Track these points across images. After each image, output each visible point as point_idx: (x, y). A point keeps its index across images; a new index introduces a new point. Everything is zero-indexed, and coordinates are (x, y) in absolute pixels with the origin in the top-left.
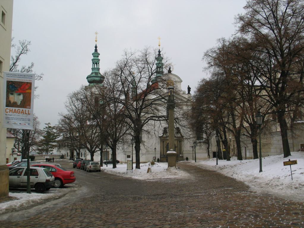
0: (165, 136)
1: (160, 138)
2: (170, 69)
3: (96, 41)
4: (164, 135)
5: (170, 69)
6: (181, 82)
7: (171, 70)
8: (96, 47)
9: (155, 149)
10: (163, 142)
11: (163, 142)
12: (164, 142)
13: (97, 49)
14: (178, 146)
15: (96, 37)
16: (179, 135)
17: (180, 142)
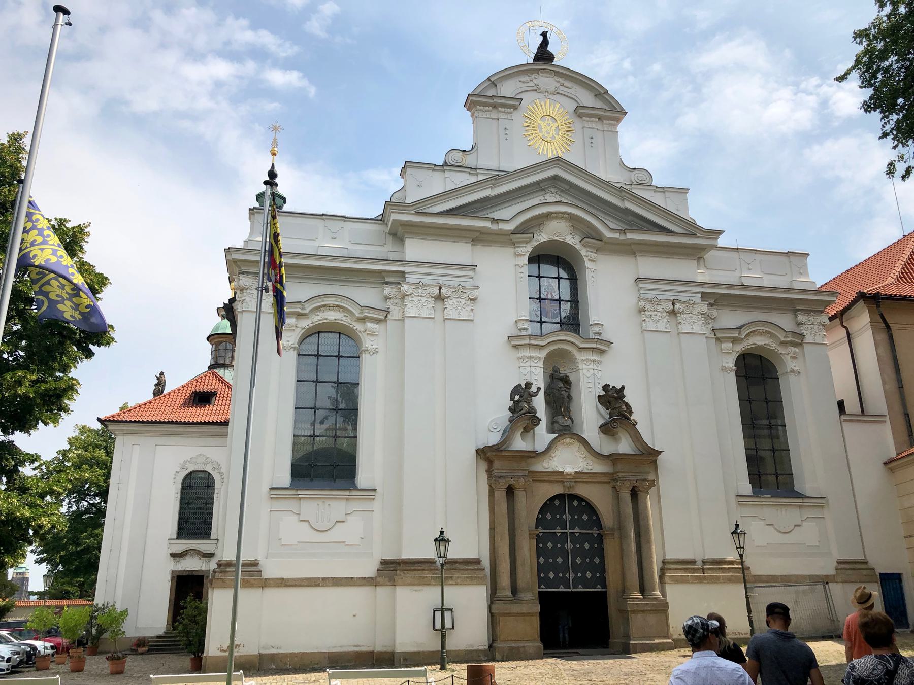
0: (519, 444)
1: (484, 466)
2: (545, 43)
3: (274, 154)
4: (518, 435)
5: (545, 43)
6: (618, 120)
7: (549, 48)
8: (272, 174)
9: (442, 540)
10: (510, 491)
11: (510, 491)
12: (520, 496)
13: (277, 180)
14: (621, 527)
15: (275, 140)
16: (625, 446)
17: (634, 493)
